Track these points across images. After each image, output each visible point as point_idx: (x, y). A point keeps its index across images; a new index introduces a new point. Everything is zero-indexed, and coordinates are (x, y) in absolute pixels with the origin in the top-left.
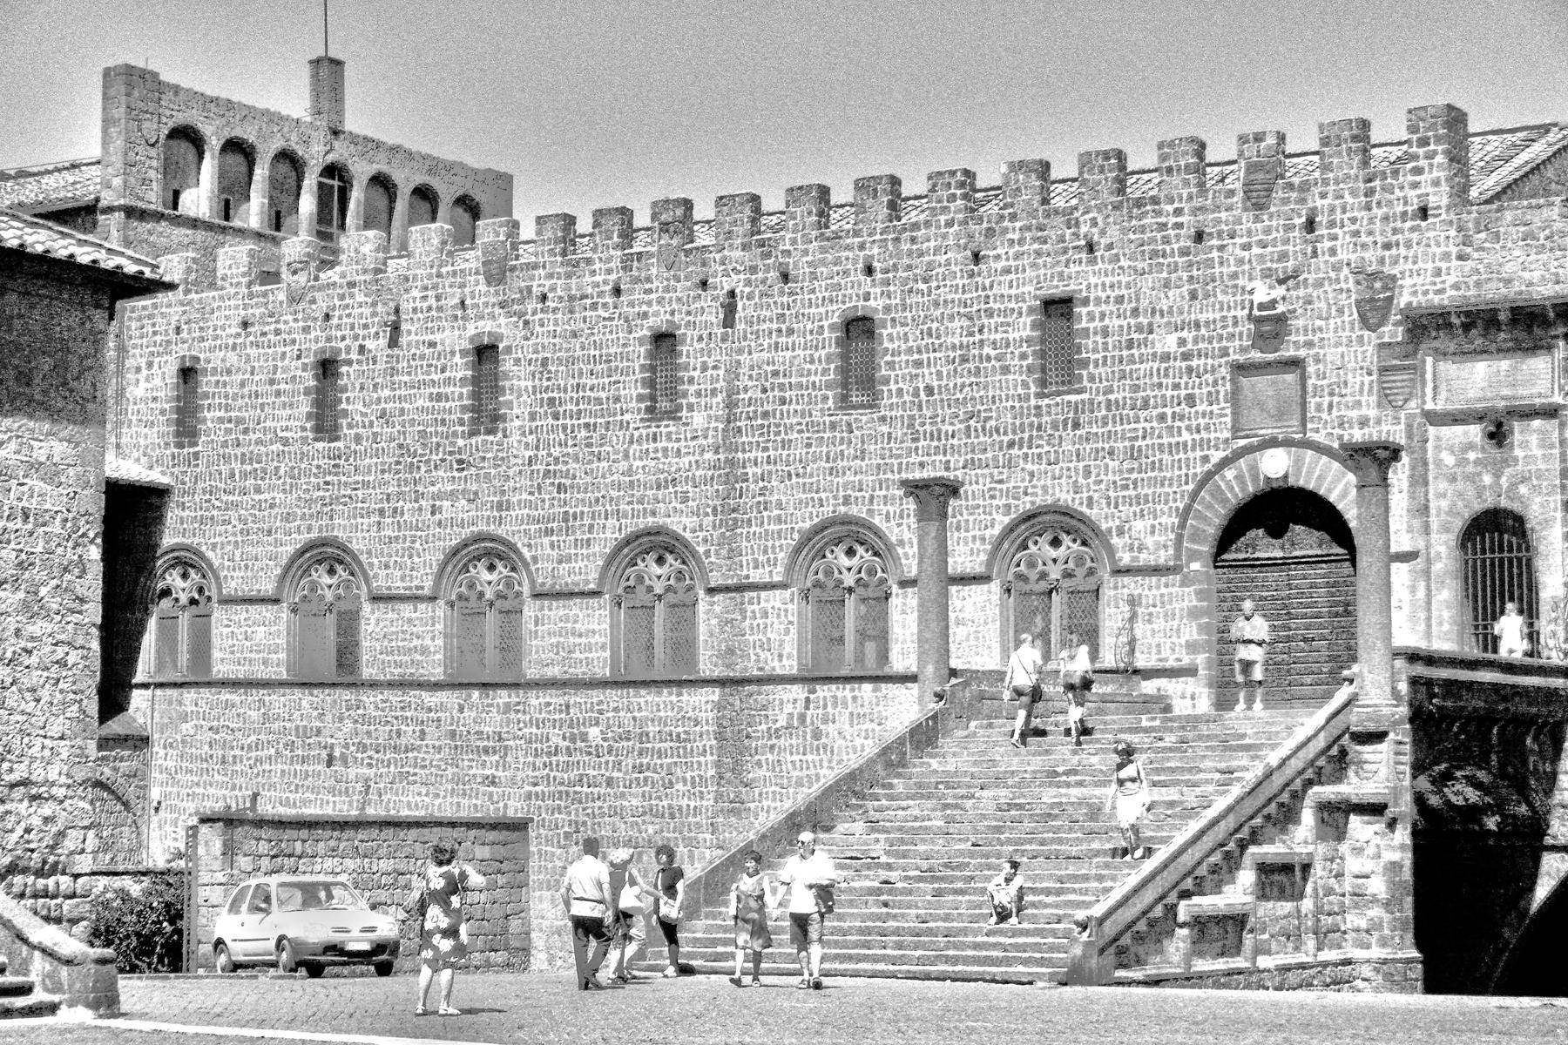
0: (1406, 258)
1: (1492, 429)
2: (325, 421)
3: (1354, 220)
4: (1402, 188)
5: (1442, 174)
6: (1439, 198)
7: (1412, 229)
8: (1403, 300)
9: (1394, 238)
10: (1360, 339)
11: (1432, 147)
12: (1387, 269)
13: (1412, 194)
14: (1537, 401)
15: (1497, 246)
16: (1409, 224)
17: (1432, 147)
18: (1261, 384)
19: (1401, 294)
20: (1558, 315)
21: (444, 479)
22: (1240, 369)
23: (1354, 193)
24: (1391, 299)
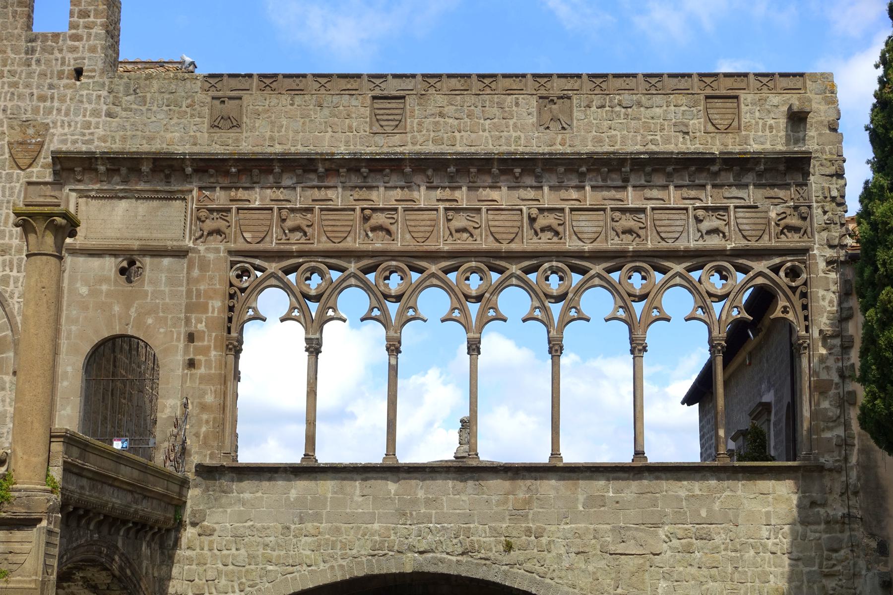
0: (59, 110)
1: (125, 264)
3: (12, 73)
4: (61, 51)
5: (99, 43)
6: (94, 62)
7: (66, 86)
8: (55, 145)
9: (49, 93)
10: (10, 177)
11: (92, 19)
12: (40, 118)
13: (69, 56)
14: (169, 243)
15: (144, 109)
16: (65, 81)
17: (92, 19)
19: (51, 141)
20: (196, 171)
23: (15, 50)
24: (42, 144)
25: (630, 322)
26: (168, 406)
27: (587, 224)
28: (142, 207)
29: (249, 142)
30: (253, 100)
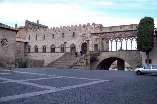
2: (36, 39)
18: (84, 37)
21: (42, 42)
22: (83, 36)
25: (126, 41)
26: (99, 48)
27: (123, 35)
28: (97, 36)
29: (102, 32)
30: (103, 29)
